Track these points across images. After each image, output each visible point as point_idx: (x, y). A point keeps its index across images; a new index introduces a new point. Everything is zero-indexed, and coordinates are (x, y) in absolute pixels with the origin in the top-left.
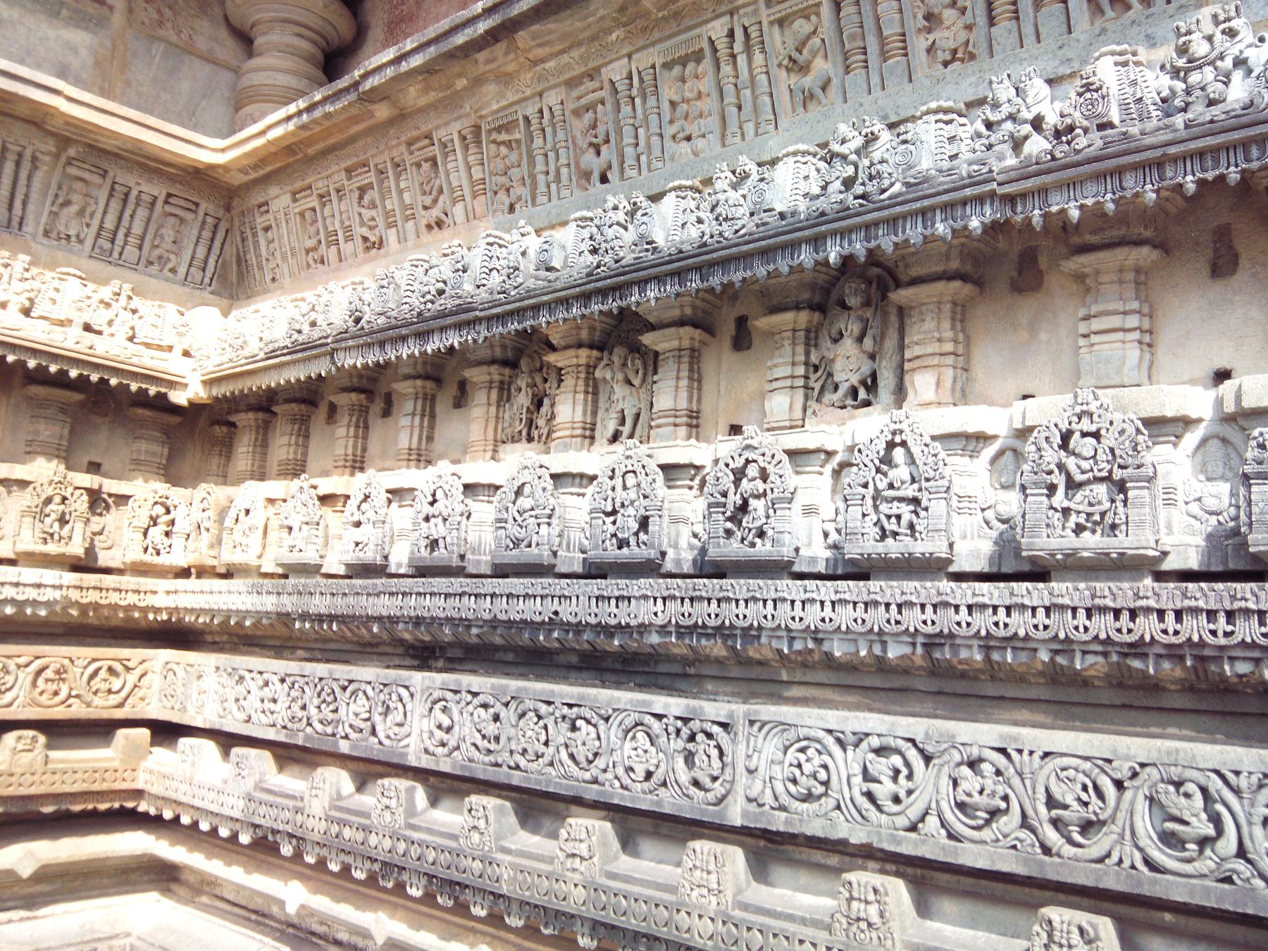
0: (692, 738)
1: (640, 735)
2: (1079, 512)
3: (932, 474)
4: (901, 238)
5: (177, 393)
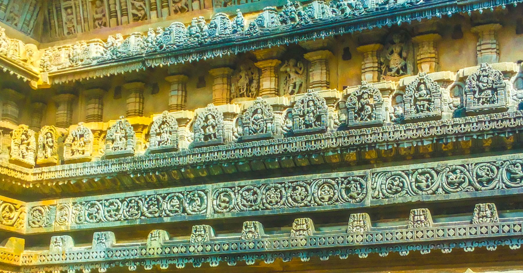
0: (349, 183)
1: (326, 186)
2: (483, 98)
3: (435, 91)
4: (424, 17)
5: (34, 82)
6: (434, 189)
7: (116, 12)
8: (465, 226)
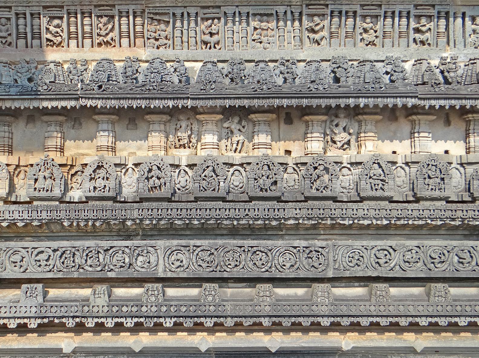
6: (392, 265)
7: (26, 33)
8: (423, 303)
